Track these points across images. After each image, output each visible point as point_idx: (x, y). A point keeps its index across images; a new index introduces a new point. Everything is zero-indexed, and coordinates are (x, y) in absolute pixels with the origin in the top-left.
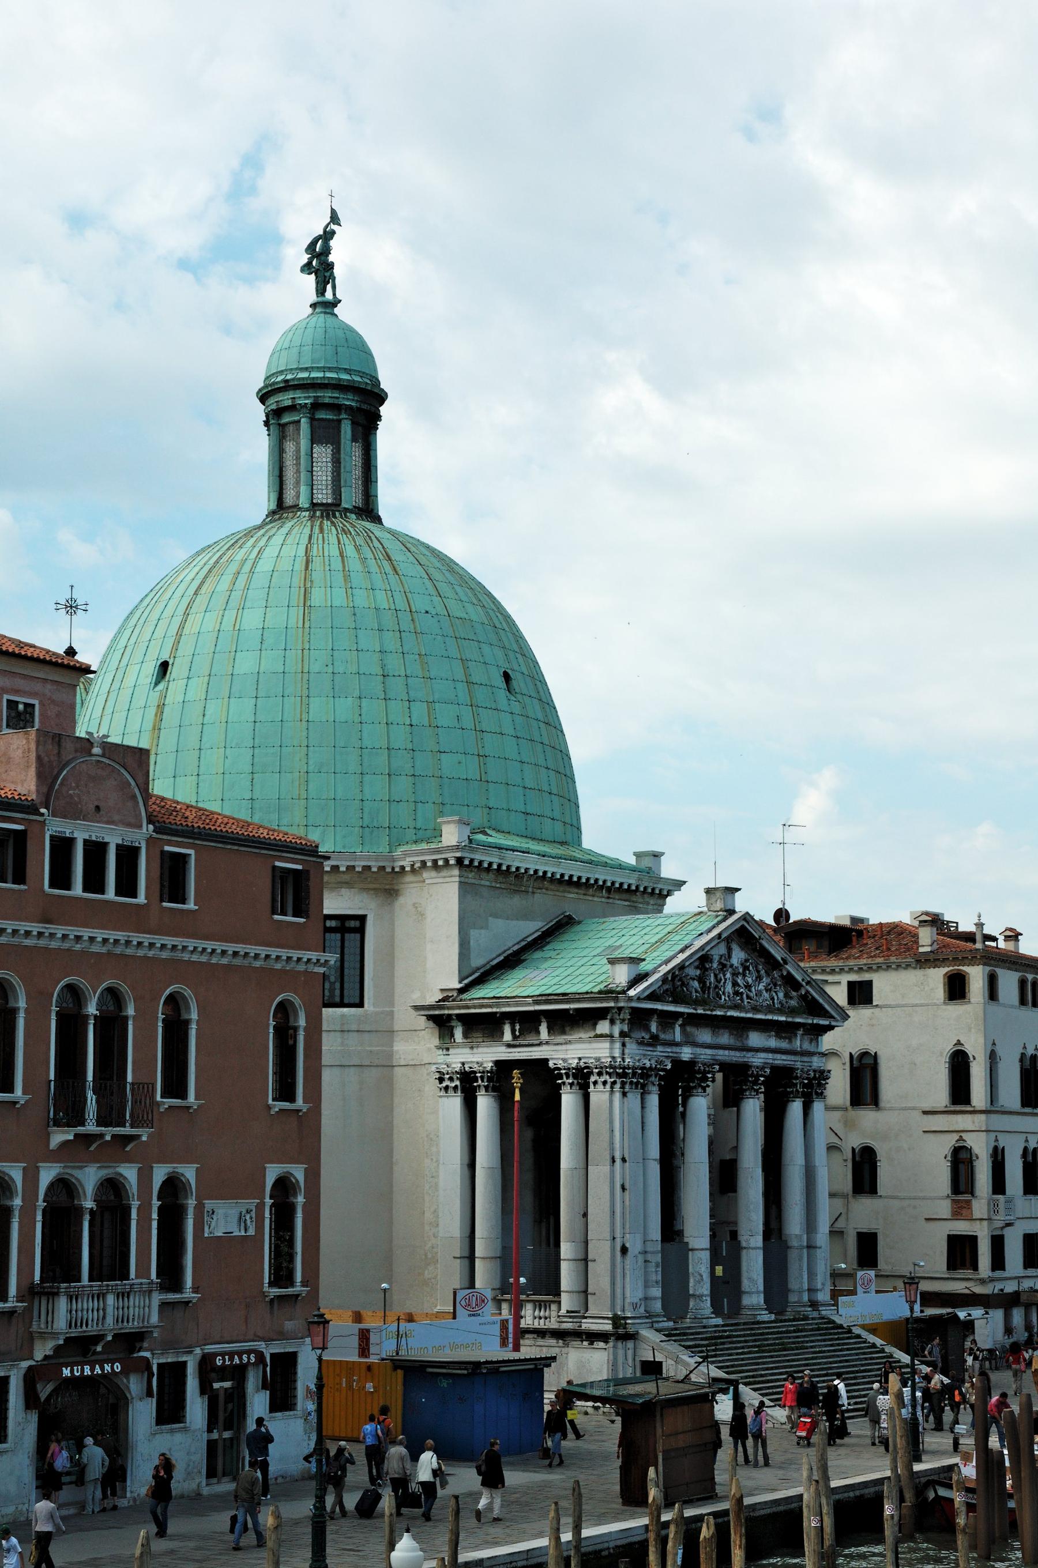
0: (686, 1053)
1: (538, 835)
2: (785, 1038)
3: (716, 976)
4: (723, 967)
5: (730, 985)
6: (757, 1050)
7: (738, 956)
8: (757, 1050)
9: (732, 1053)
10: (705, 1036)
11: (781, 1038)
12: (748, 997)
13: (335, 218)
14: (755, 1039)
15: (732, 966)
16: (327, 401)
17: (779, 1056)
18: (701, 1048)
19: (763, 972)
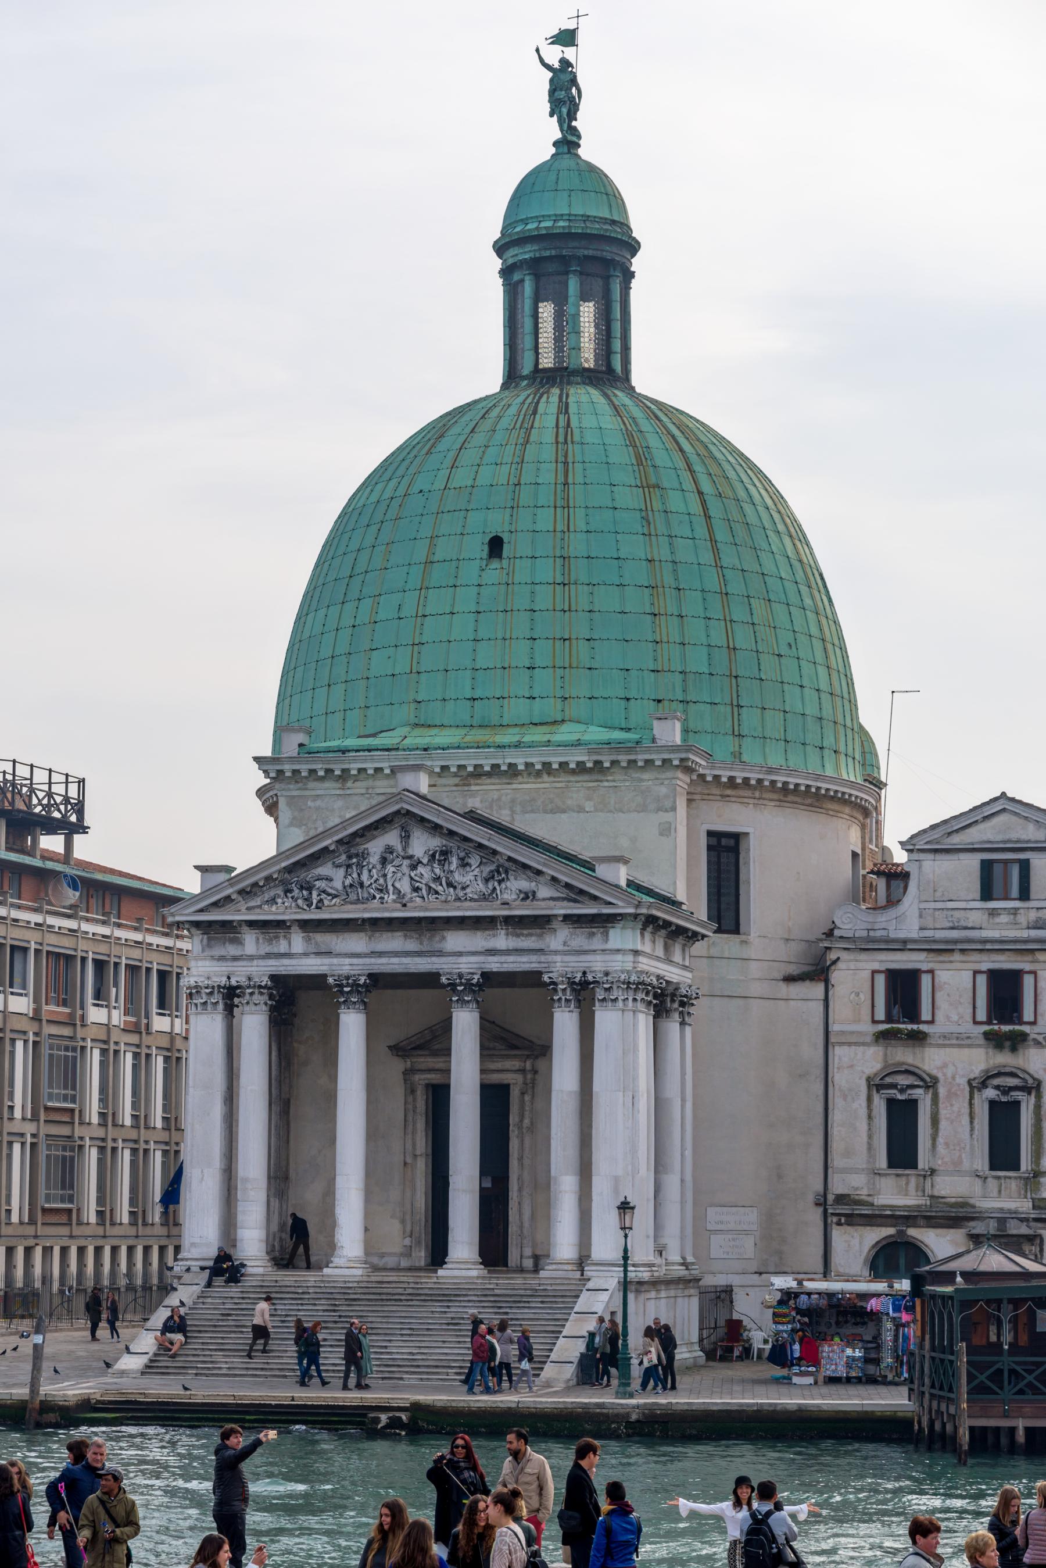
0: (311, 966)
1: (495, 720)
2: (531, 935)
3: (370, 871)
4: (384, 861)
5: (406, 879)
6: (460, 954)
7: (421, 844)
8: (460, 954)
9: (405, 960)
10: (356, 942)
11: (518, 936)
12: (437, 893)
13: (537, 50)
14: (455, 940)
15: (411, 857)
16: (510, 261)
17: (511, 959)
18: (347, 957)
19: (474, 860)
